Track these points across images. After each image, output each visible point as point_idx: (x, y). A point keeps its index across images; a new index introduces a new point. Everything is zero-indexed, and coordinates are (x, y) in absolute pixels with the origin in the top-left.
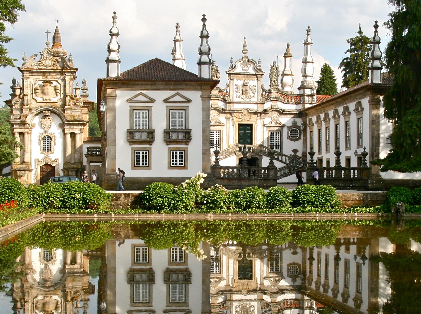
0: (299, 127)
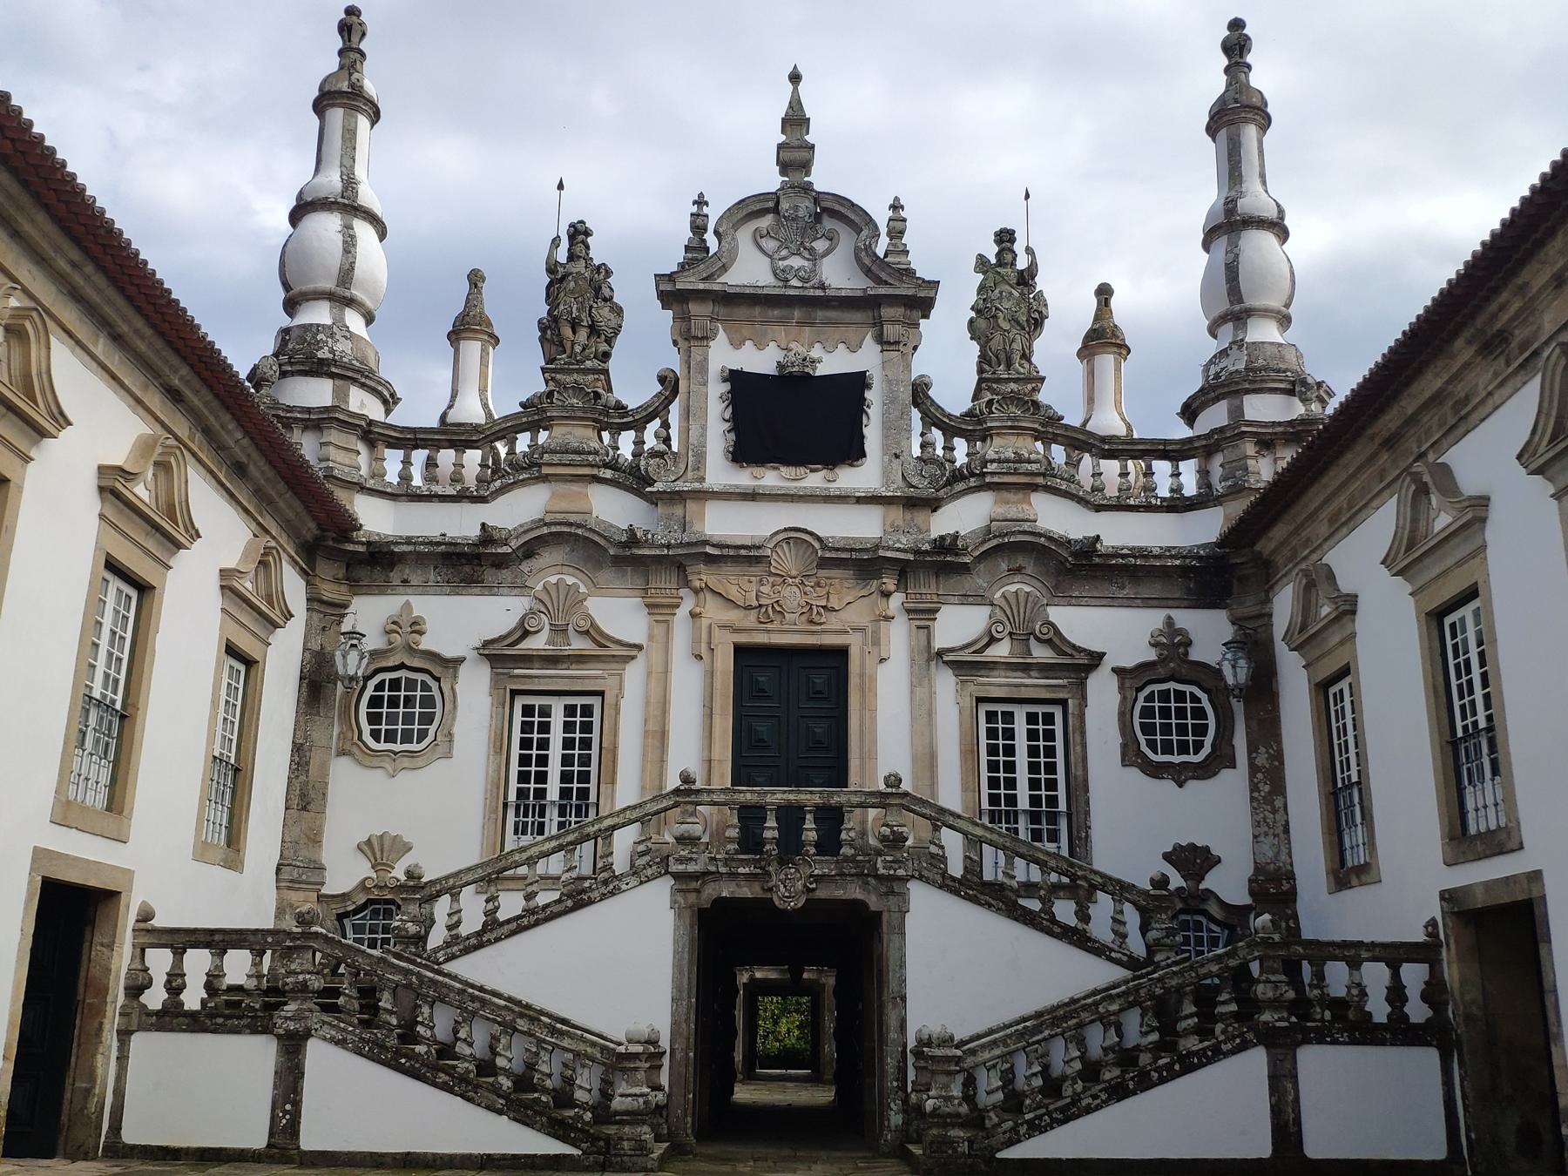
0: (1207, 676)
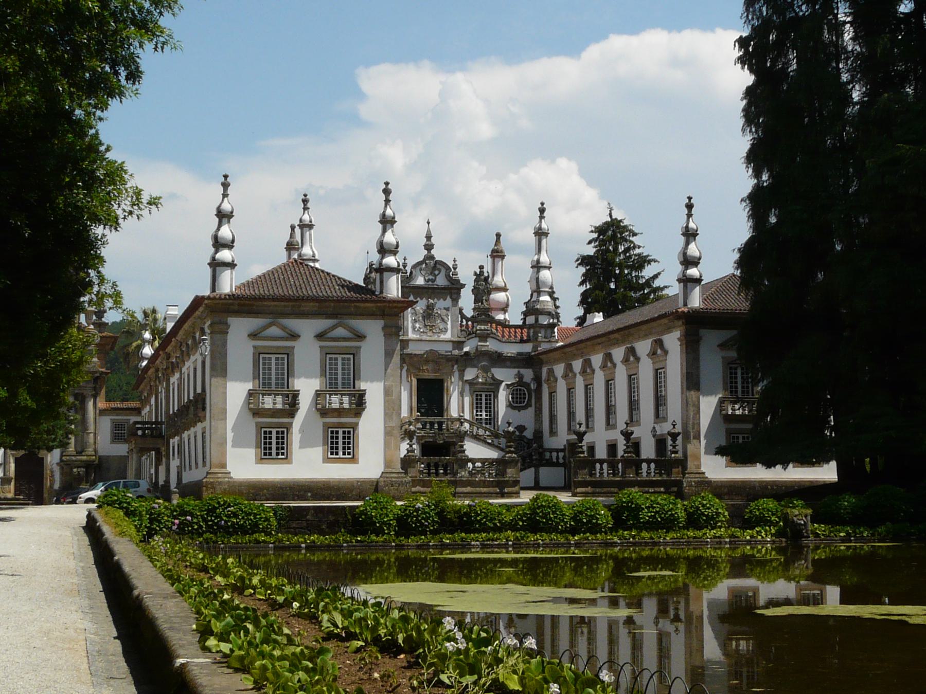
0: (527, 385)
